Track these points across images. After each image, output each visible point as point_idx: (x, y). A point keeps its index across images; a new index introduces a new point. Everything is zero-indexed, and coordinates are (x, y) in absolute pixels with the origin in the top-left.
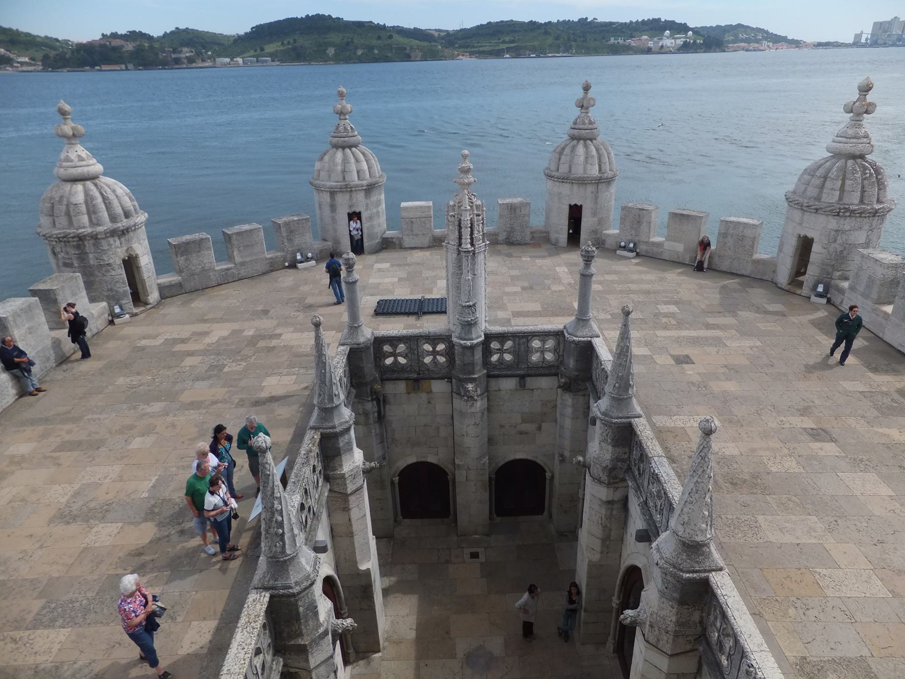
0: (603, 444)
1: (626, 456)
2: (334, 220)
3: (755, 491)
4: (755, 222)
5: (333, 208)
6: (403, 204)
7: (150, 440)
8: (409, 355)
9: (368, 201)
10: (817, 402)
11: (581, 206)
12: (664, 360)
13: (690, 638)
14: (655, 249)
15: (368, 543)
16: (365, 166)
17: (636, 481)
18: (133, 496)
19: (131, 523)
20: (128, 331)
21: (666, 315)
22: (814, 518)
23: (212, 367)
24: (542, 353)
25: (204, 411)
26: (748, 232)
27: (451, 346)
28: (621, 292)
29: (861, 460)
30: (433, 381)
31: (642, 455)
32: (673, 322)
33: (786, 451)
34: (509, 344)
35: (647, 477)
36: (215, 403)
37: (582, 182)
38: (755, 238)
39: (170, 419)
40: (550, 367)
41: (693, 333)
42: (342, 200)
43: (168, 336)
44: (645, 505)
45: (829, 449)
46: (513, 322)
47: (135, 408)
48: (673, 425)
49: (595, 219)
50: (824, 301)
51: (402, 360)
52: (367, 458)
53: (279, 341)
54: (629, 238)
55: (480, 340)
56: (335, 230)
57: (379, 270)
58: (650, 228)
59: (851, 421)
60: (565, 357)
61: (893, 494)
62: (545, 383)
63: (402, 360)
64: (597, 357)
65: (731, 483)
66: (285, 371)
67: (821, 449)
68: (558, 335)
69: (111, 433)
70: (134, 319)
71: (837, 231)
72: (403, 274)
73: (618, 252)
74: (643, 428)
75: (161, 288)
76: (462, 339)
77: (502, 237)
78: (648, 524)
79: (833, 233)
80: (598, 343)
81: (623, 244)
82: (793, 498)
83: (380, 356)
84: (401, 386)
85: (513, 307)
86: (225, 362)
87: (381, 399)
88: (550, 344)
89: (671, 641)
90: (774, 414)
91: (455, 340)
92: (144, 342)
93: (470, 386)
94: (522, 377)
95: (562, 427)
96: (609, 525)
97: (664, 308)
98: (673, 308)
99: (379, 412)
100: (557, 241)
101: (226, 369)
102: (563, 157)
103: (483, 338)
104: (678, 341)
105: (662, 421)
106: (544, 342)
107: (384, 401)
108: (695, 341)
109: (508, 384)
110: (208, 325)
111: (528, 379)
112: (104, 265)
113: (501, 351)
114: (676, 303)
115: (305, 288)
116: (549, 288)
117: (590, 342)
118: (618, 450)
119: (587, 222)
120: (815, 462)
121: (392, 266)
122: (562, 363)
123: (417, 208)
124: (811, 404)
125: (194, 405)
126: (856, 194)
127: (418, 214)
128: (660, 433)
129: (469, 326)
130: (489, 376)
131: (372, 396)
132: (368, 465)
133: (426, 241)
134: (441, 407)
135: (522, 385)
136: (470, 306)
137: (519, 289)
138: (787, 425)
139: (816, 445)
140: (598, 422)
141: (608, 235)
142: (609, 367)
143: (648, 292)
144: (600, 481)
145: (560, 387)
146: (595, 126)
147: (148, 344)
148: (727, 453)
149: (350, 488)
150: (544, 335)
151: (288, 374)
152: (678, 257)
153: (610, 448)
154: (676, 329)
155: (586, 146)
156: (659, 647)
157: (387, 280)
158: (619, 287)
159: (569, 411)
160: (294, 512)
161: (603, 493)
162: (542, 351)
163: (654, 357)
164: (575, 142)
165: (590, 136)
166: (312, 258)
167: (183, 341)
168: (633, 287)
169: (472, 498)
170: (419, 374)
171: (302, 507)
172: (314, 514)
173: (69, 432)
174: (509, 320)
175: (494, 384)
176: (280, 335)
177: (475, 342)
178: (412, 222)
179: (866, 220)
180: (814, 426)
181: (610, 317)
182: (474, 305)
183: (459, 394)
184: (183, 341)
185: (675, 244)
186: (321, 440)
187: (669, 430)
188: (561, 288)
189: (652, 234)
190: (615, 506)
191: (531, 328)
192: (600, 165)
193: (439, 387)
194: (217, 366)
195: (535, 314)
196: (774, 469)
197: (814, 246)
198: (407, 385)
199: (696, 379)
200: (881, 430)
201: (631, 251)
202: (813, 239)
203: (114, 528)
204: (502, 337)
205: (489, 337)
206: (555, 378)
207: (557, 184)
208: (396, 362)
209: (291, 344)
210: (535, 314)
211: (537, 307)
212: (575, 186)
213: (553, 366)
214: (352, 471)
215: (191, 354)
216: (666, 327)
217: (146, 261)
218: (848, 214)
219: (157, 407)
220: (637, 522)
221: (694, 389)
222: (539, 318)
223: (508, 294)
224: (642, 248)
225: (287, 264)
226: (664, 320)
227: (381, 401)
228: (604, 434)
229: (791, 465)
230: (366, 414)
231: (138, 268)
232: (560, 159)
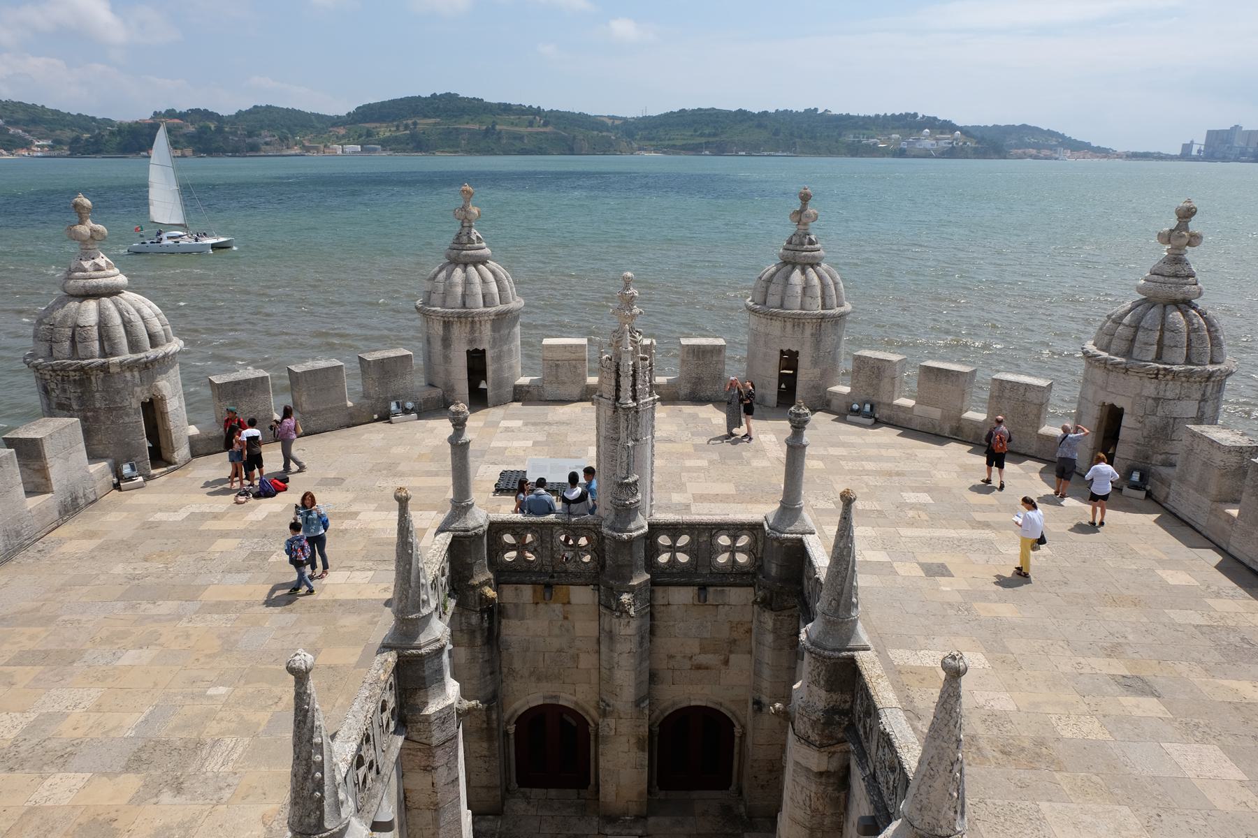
0: (814, 688)
1: (847, 706)
2: (447, 359)
3: (1038, 765)
4: (1043, 383)
5: (446, 342)
6: (546, 341)
7: (147, 654)
9: (497, 335)
10: (1130, 637)
11: (797, 353)
12: (909, 570)
14: (902, 415)
15: (459, 821)
16: (494, 288)
17: (860, 743)
18: (112, 734)
19: (105, 774)
20: (138, 498)
21: (913, 507)
22: (1125, 810)
23: (253, 554)
24: (731, 554)
25: (234, 616)
26: (1031, 396)
27: (602, 538)
28: (851, 472)
29: (1197, 726)
31: (868, 706)
32: (924, 516)
33: (1086, 708)
34: (684, 540)
35: (875, 737)
37: (798, 321)
38: (1041, 405)
39: (183, 624)
41: (952, 533)
42: (460, 334)
43: (195, 509)
44: (872, 780)
45: (1148, 707)
46: (693, 509)
47: (133, 607)
48: (918, 663)
49: (817, 371)
50: (1142, 494)
51: (531, 557)
52: (464, 694)
53: (354, 522)
54: (864, 397)
55: (641, 531)
56: (448, 373)
57: (507, 429)
58: (893, 385)
59: (1182, 667)
60: (766, 560)
61: (1245, 778)
62: (739, 596)
63: (531, 557)
64: (810, 562)
65: (1003, 752)
66: (358, 565)
67: (1138, 707)
68: (754, 528)
69: (93, 640)
70: (149, 483)
71: (1157, 399)
72: (541, 437)
73: (849, 418)
74: (868, 663)
75: (193, 441)
76: (614, 530)
77: (685, 390)
78: (876, 808)
79: (1150, 401)
80: (809, 540)
81: (856, 407)
82: (1094, 778)
83: (496, 548)
84: (527, 592)
85: (694, 488)
86: (273, 549)
87: (496, 610)
88: (743, 541)
90: (1068, 653)
91: (605, 530)
92: (160, 516)
93: (625, 598)
94: (703, 588)
95: (758, 662)
96: (821, 808)
97: (911, 497)
98: (925, 498)
99: (490, 629)
100: (763, 398)
101: (273, 558)
102: (772, 288)
103: (646, 529)
104: (931, 543)
105: (900, 656)
106: (735, 538)
108: (956, 545)
109: (682, 596)
111: (711, 589)
112: (115, 409)
113: (673, 549)
114: (928, 490)
115: (398, 450)
116: (749, 463)
117: (801, 540)
118: (835, 697)
119: (806, 375)
120: (1127, 726)
121: (526, 424)
122: (760, 568)
123: (565, 346)
124: (1122, 640)
125: (221, 607)
126: (1179, 350)
127: (567, 355)
128: (896, 673)
129: (626, 512)
130: (653, 583)
131: (481, 604)
132: (466, 704)
133: (576, 391)
134: (585, 627)
136: (628, 484)
137: (704, 463)
138: (1087, 670)
139: (1130, 701)
140: (806, 655)
141: (835, 394)
142: (822, 575)
143: (890, 474)
144: (807, 741)
145: (755, 602)
146: (818, 246)
147: (164, 518)
148: (997, 707)
149: (437, 737)
150: (735, 529)
151: (364, 569)
152: (934, 426)
153: (823, 693)
154: (928, 527)
155: (803, 272)
157: (516, 444)
158: (847, 465)
159: (769, 638)
160: (343, 767)
161: (815, 760)
162: (732, 550)
163: (895, 565)
164: (789, 267)
165: (810, 261)
166: (413, 410)
167: (216, 516)
168: (869, 466)
169: (622, 765)
171: (359, 761)
172: (378, 773)
173: (32, 638)
174: (687, 507)
176: (357, 514)
177: (635, 534)
178: (557, 365)
179: (1196, 386)
180: (1127, 673)
182: (635, 483)
183: (608, 607)
184: (216, 516)
185: (929, 408)
186: (397, 665)
187: (913, 671)
188: (765, 463)
189: (896, 394)
191: (717, 518)
192: (823, 298)
193: (582, 596)
194: (261, 554)
195: (725, 498)
196: (1067, 734)
197: (1125, 417)
198: (535, 591)
199: (958, 598)
200: (1226, 682)
202: (1122, 409)
203: (75, 780)
204: (674, 529)
205: (656, 529)
206: (751, 590)
207: (764, 321)
209: (371, 526)
210: (725, 498)
211: (729, 489)
212: (789, 325)
213: (747, 573)
214: (440, 711)
215: (225, 534)
216: (912, 524)
217: (175, 406)
218: (1169, 377)
219: (166, 607)
220: (861, 806)
221: (951, 612)
222: (732, 505)
223: (689, 470)
224: (881, 413)
225: (376, 417)
226: (911, 513)
227: (494, 612)
228: (815, 673)
229: (1093, 730)
230: (472, 633)
231: (164, 414)
232: (767, 288)
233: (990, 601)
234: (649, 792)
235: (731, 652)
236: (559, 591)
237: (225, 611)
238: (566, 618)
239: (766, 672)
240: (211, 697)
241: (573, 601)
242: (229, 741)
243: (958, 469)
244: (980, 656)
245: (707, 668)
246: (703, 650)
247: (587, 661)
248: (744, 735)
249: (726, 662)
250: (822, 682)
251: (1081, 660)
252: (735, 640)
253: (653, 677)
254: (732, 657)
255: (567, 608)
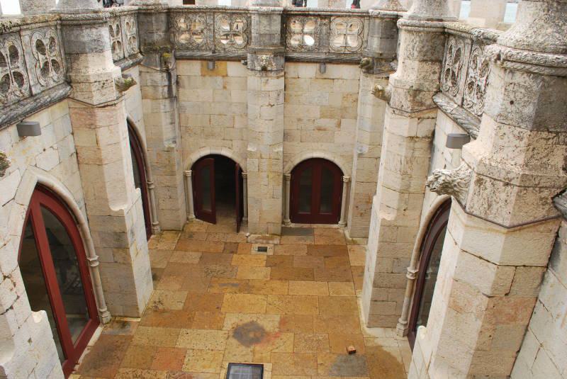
8: (205, 31)
13: (546, 193)
30: (228, 63)
40: (353, 53)
89: (513, 198)
103: (281, 9)
107: (177, 83)
109: (307, 72)
135: (323, 71)
153: (416, 64)
156: (490, 217)
170: (214, 52)
175: (292, 69)
190: (418, 145)
193: (233, 69)
208: (190, 41)
228: (410, 47)
234: (283, 223)
235: (343, 117)
236: (221, 66)
238: (225, 88)
241: (229, 74)
245: (325, 130)
246: (323, 116)
247: (238, 124)
248: (350, 181)
249: (339, 125)
250: (416, 54)
252: (345, 108)
253: (286, 136)
254: (343, 120)
255: (226, 79)
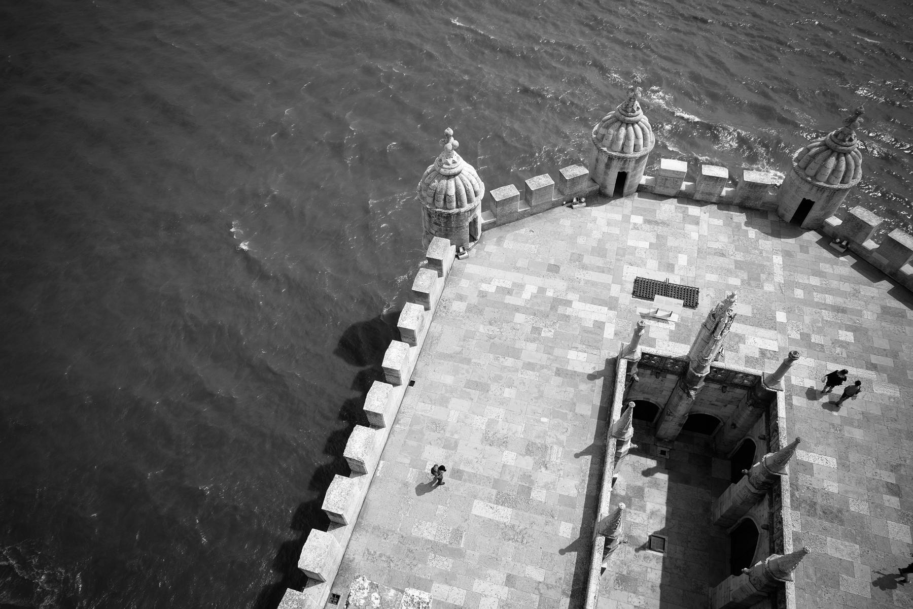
2: (606, 173)
5: (608, 166)
36: (542, 367)
56: (605, 180)
66: (580, 346)
72: (654, 241)
110: (521, 275)
127: (674, 175)
167: (509, 292)
181: (798, 337)
201: (842, 247)
233: (853, 426)
237: (533, 370)
239: (742, 419)
240: (543, 423)
242: (555, 447)
243: (879, 311)
244: (835, 460)
251: (878, 471)
